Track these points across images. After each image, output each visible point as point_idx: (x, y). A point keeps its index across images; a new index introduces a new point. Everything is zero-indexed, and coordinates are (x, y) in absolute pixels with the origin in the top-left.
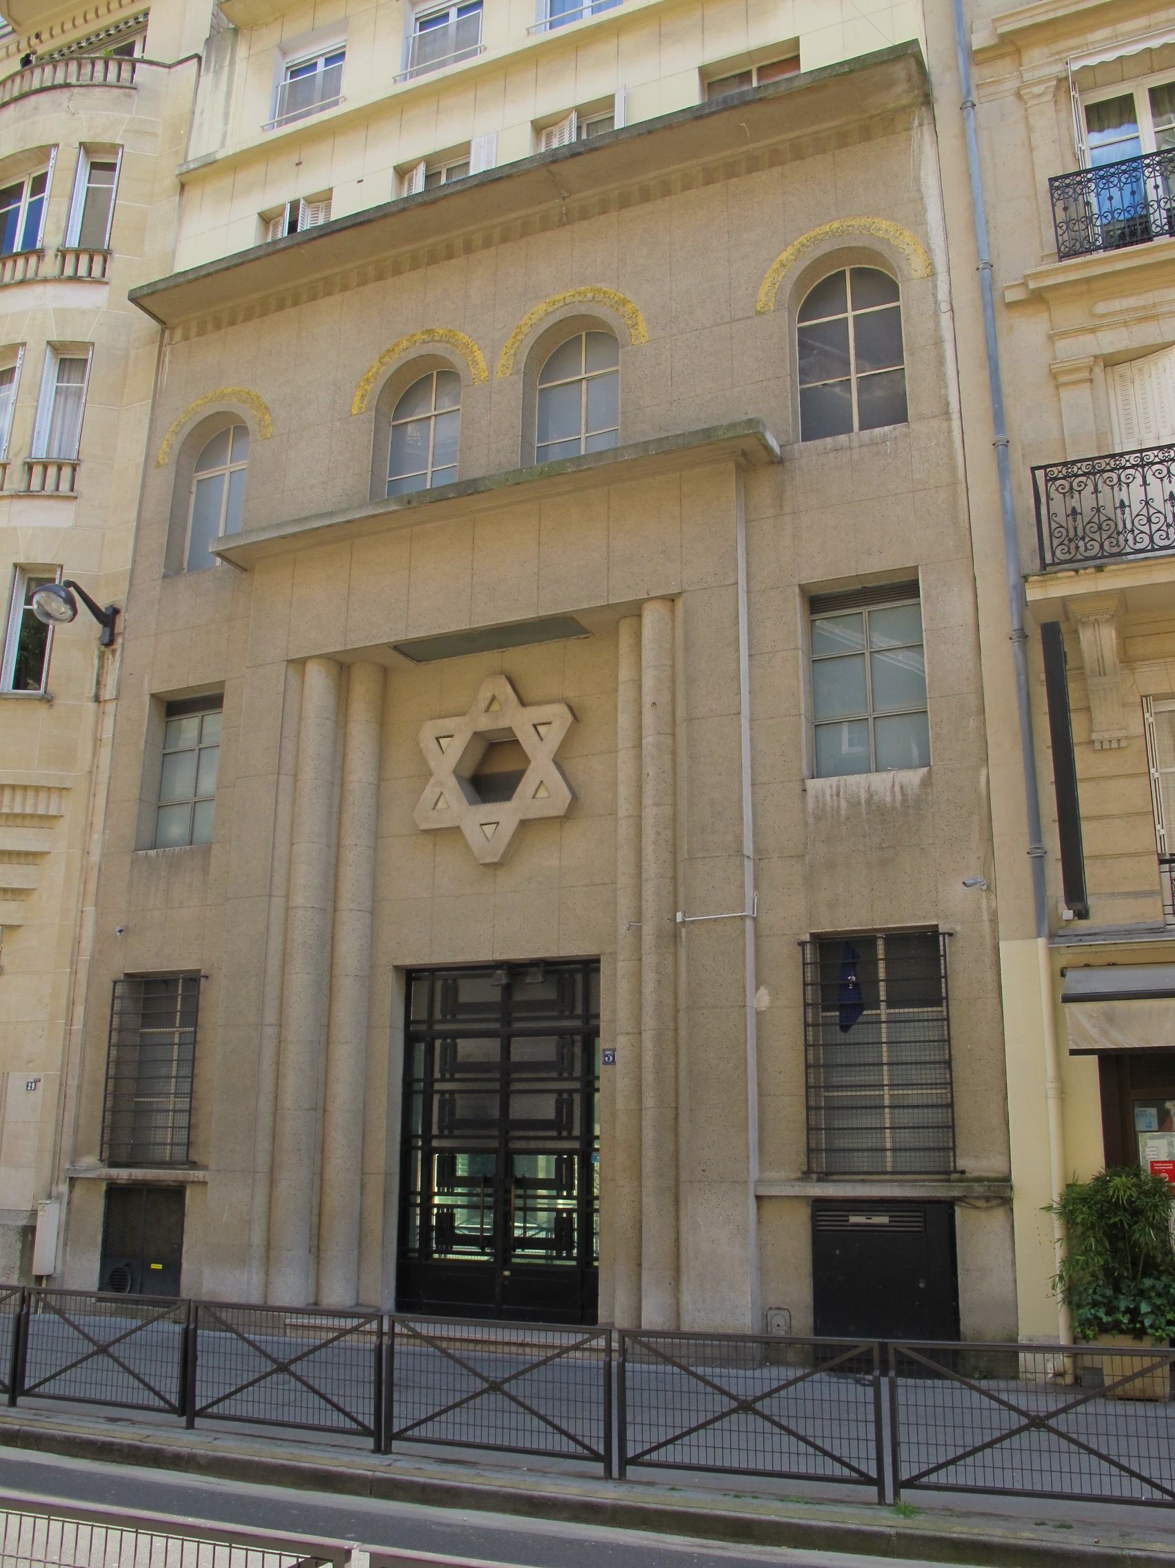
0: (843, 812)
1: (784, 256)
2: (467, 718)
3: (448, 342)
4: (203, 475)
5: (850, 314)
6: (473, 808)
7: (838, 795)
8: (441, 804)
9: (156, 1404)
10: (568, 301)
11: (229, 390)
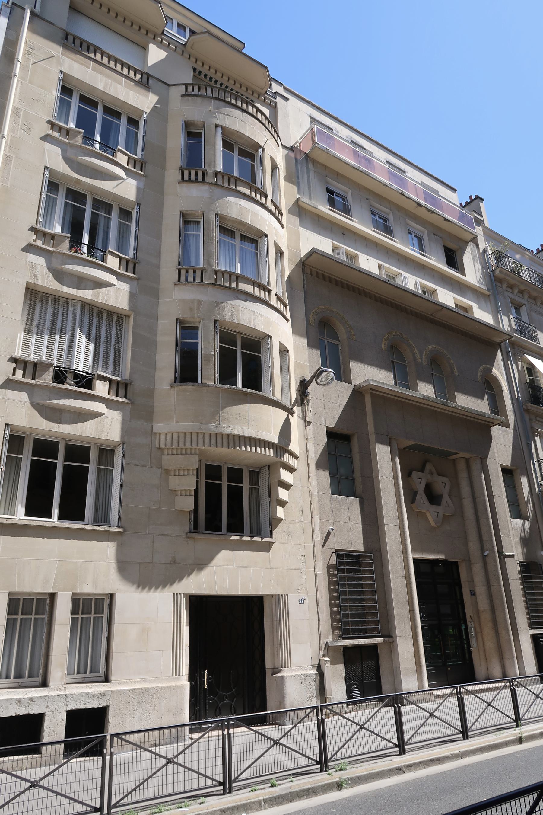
9: (211, 783)
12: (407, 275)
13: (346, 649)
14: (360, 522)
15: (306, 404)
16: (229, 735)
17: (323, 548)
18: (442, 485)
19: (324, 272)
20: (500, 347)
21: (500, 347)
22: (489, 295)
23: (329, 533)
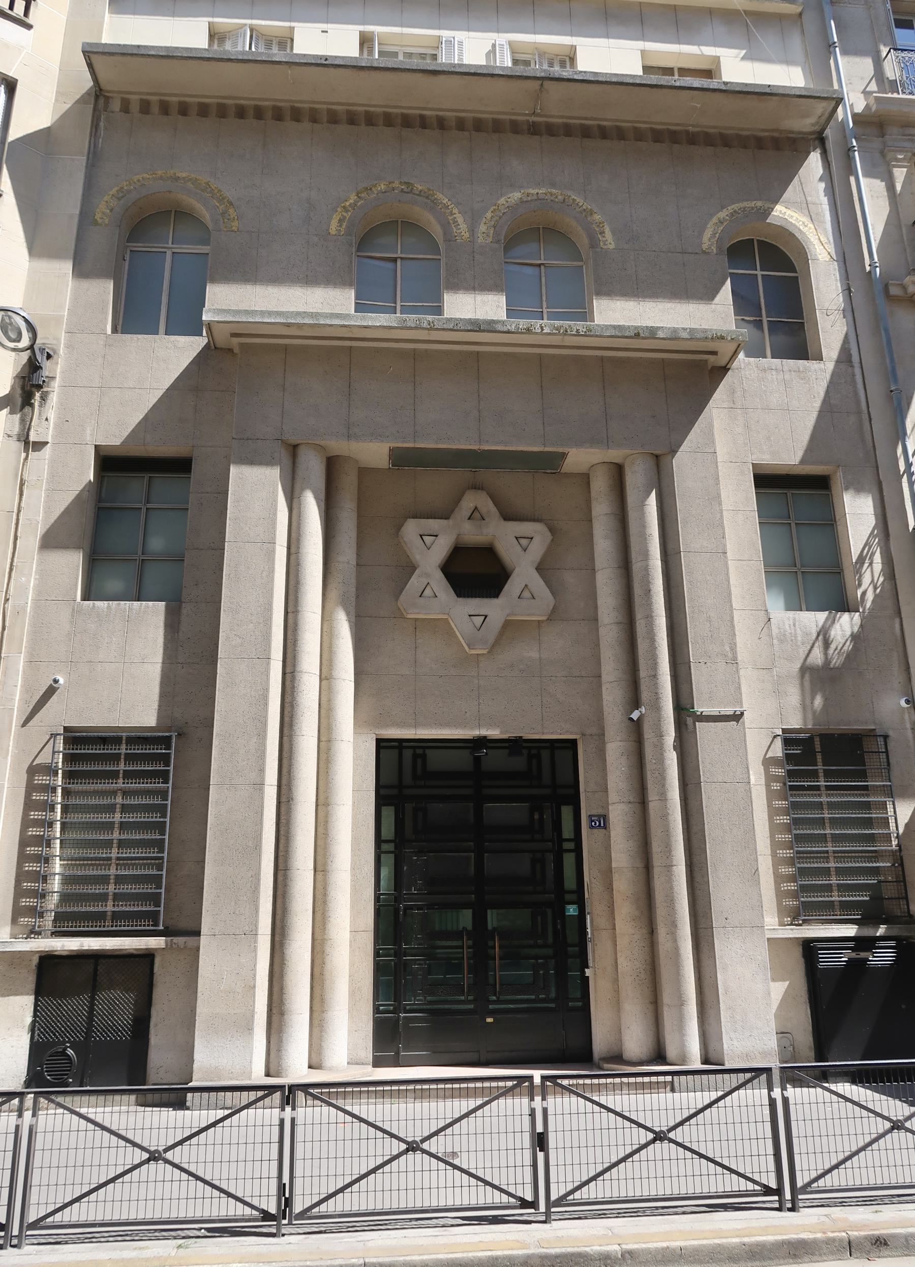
0: (799, 638)
1: (722, 215)
2: (451, 522)
3: (427, 198)
4: (139, 246)
5: (759, 273)
7: (794, 625)
8: (428, 592)
10: (541, 196)
11: (184, 175)
12: (460, 35)
13: (47, 961)
14: (159, 658)
15: (37, 404)
17: (24, 725)
18: (521, 548)
19: (165, 95)
20: (820, 140)
21: (820, 140)
22: (800, 14)
23: (51, 691)
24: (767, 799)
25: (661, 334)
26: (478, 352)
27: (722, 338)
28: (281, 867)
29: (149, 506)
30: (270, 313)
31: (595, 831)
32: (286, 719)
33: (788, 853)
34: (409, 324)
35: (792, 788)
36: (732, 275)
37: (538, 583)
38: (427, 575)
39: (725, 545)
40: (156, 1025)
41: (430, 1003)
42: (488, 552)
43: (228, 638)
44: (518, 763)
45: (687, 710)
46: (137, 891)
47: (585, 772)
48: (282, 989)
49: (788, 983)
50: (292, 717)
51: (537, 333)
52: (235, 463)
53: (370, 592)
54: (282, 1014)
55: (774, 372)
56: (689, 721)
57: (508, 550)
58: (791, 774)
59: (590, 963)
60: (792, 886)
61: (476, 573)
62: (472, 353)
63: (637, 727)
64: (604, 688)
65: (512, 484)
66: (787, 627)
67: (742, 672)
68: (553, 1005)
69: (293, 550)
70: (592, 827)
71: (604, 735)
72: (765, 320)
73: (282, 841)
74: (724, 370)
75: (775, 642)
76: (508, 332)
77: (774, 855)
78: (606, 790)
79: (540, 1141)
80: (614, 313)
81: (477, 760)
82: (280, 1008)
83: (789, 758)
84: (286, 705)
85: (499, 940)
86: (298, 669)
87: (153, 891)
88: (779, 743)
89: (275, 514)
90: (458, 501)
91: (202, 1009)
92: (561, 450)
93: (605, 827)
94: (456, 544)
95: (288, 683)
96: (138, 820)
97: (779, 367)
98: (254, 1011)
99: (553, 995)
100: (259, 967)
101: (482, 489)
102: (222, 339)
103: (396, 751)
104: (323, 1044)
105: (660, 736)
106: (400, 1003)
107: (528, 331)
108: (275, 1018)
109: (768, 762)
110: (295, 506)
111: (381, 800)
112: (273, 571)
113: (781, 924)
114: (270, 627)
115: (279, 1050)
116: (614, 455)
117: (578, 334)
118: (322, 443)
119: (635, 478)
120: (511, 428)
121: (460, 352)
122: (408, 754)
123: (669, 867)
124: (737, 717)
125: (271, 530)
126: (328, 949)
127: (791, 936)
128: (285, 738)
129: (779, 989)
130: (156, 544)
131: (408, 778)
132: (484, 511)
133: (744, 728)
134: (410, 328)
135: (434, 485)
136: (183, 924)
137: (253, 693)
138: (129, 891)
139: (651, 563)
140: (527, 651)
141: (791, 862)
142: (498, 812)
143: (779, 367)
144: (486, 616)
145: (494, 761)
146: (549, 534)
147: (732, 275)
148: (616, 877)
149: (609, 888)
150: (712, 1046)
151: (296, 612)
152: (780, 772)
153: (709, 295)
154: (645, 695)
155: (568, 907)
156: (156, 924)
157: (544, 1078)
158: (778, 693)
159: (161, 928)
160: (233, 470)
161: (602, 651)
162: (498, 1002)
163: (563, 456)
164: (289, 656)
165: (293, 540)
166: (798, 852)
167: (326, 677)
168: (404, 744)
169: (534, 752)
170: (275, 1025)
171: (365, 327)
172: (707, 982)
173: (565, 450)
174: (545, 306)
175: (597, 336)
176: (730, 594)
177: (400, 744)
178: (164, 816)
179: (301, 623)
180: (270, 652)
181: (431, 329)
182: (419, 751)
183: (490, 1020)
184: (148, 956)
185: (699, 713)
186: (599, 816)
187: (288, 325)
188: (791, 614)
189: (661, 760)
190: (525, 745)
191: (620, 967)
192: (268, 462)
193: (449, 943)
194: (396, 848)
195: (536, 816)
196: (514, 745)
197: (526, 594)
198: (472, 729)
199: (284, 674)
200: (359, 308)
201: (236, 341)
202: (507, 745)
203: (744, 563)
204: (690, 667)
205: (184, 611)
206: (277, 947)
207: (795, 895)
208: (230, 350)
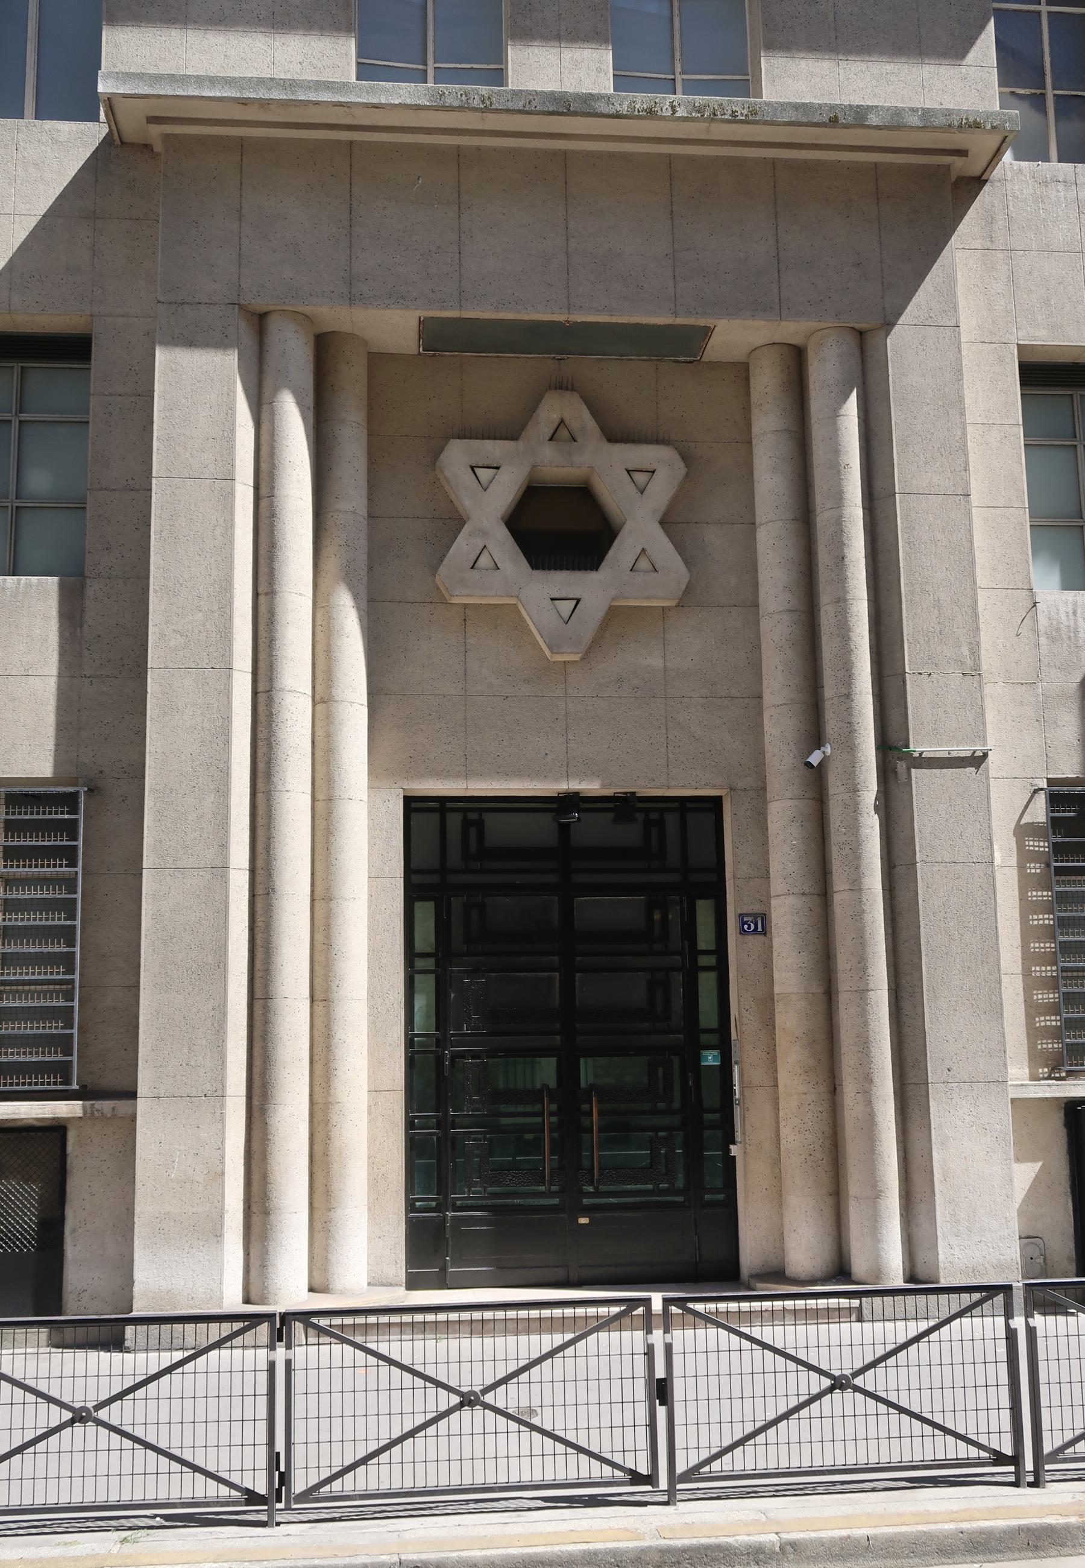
2: (520, 445)
5: (1044, 9)
6: (538, 573)
7: (1075, 613)
8: (484, 561)
14: (51, 666)
16: (1031, 1332)
18: (635, 485)
24: (1020, 888)
25: (873, 119)
26: (565, 152)
27: (977, 125)
28: (258, 994)
29: (24, 417)
30: (213, 81)
31: (749, 938)
32: (261, 766)
33: (1049, 970)
34: (449, 101)
35: (1059, 871)
36: (998, 13)
37: (662, 547)
38: (484, 533)
39: (968, 483)
40: (74, 1231)
41: (495, 1195)
42: (582, 494)
43: (162, 636)
44: (630, 834)
45: (898, 749)
46: (35, 1031)
47: (735, 847)
48: (265, 1177)
49: (1040, 1164)
50: (269, 762)
51: (664, 118)
52: (161, 343)
53: (390, 559)
54: (266, 1213)
55: (1061, 187)
56: (901, 766)
57: (614, 492)
58: (1058, 850)
59: (738, 1136)
60: (1053, 1021)
61: (562, 529)
62: (555, 153)
63: (817, 777)
64: (766, 716)
65: (621, 380)
66: (1063, 617)
67: (987, 690)
68: (680, 1199)
69: (264, 491)
70: (743, 932)
71: (764, 789)
72: (1050, 93)
73: (259, 955)
74: (979, 182)
75: (1043, 640)
76: (617, 116)
77: (1026, 973)
78: (767, 876)
79: (661, 1391)
80: (797, 82)
81: (564, 829)
82: (264, 1204)
83: (1056, 824)
84: (260, 743)
85: (599, 1102)
86: (277, 686)
87: (60, 1031)
88: (1041, 800)
89: (233, 431)
90: (532, 409)
91: (144, 1207)
92: (702, 322)
93: (764, 932)
94: (530, 482)
95: (261, 708)
96: (32, 923)
97: (1071, 177)
98: (223, 1208)
99: (680, 1183)
100: (228, 1144)
101: (573, 390)
102: (132, 126)
103: (435, 817)
104: (330, 1256)
105: (854, 790)
106: (446, 1197)
107: (650, 113)
108: (256, 1219)
109: (1023, 831)
110: (265, 417)
111: (413, 893)
112: (232, 526)
113: (1034, 1077)
114: (231, 619)
115: (263, 1266)
116: (790, 330)
117: (734, 120)
118: (308, 310)
119: (825, 368)
120: (620, 280)
121: (537, 153)
122: (454, 821)
123: (862, 992)
124: (977, 761)
125: (224, 455)
126: (334, 1118)
127: (1048, 1095)
128: (260, 796)
129: (1025, 1174)
130: (40, 481)
131: (454, 858)
132: (575, 426)
133: (988, 778)
134: (451, 109)
135: (495, 382)
136: (111, 1080)
137: (206, 725)
138: (22, 1032)
139: (847, 512)
140: (645, 657)
141: (1053, 984)
142: (595, 910)
143: (1071, 177)
144: (578, 601)
145: (590, 830)
146: (682, 465)
147: (998, 13)
148: (779, 1007)
149: (769, 1024)
150: (922, 1256)
151: (272, 593)
152: (1042, 846)
153: (956, 48)
154: (832, 726)
155: (705, 1053)
156: (67, 1081)
157: (667, 1302)
158: (1043, 721)
159: (75, 1087)
160: (162, 356)
161: (764, 657)
162: (597, 1194)
163: (706, 332)
164: (262, 664)
165: (264, 476)
166: (1065, 970)
167: (323, 698)
168: (449, 805)
169: (654, 816)
170: (255, 1230)
171: (376, 106)
172: (916, 1163)
173: (708, 322)
174: (678, 69)
175: (766, 123)
176: (973, 563)
177: (442, 804)
178: (73, 917)
179: (279, 611)
180: (231, 656)
181: (486, 110)
182: (472, 816)
183: (583, 1221)
184: (57, 1130)
185: (916, 755)
186: (755, 916)
187: (244, 102)
188: (1070, 595)
189: (854, 827)
190: (639, 805)
191: (783, 1141)
192: (220, 343)
193: (521, 1109)
194: (437, 965)
195: (657, 916)
196: (623, 806)
197: (644, 564)
198: (556, 780)
199: (255, 693)
200: (364, 72)
201: (156, 130)
202: (611, 805)
203: (998, 511)
204: (904, 682)
205: (90, 592)
206: (256, 1114)
207: (1056, 1034)
208: (147, 147)
